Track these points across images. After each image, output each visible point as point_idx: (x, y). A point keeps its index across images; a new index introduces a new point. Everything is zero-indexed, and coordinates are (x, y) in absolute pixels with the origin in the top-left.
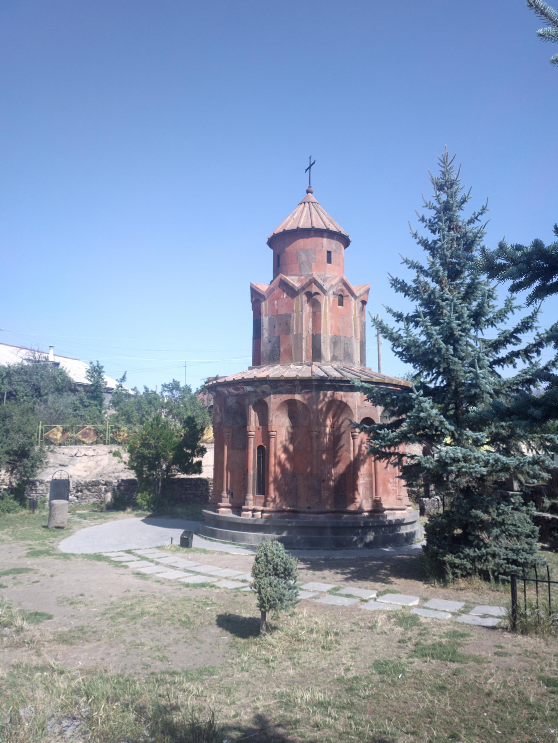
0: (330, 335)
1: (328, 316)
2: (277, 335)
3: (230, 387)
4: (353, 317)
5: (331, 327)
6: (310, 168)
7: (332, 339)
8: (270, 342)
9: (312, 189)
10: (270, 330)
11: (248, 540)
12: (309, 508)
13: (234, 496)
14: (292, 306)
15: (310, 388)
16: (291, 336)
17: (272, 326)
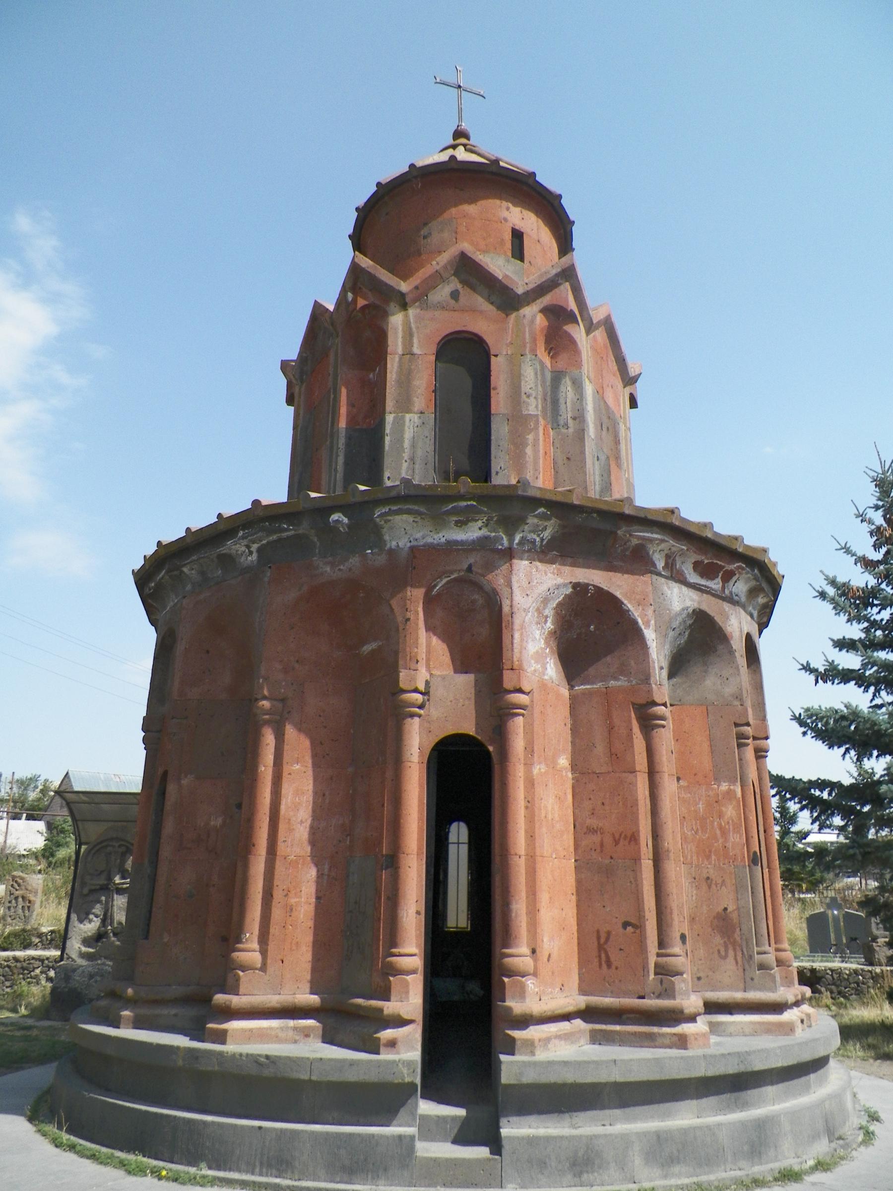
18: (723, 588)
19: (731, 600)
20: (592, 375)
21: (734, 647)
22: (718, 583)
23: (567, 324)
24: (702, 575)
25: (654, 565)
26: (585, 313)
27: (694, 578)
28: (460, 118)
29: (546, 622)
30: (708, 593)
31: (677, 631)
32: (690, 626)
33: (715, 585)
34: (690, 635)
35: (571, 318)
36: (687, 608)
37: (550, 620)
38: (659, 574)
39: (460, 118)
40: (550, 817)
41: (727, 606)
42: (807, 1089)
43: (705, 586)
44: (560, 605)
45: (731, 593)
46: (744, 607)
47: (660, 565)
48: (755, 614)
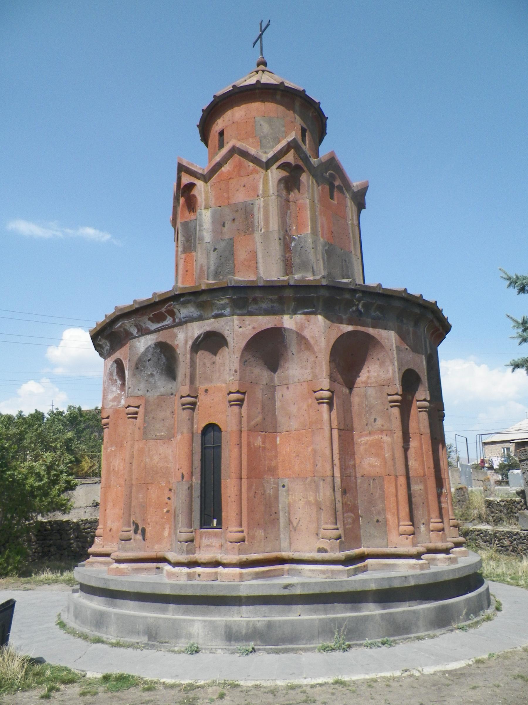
0: (322, 240)
1: (318, 209)
2: (227, 237)
3: (143, 315)
4: (350, 222)
5: (322, 227)
6: (260, 36)
7: (324, 246)
8: (215, 249)
9: (266, 59)
10: (214, 231)
11: (189, 636)
12: (320, 550)
13: (148, 535)
14: (255, 189)
15: (314, 307)
16: (257, 237)
17: (219, 223)
18: (174, 320)
19: (181, 324)
20: (212, 202)
21: (179, 352)
22: (170, 319)
23: (191, 191)
24: (158, 322)
25: (132, 334)
26: (199, 176)
27: (153, 326)
28: (262, 54)
29: (117, 382)
30: (162, 330)
31: (155, 359)
32: (161, 352)
33: (169, 321)
34: (165, 356)
35: (191, 186)
36: (150, 346)
37: (118, 380)
38: (135, 337)
39: (262, 54)
40: (116, 469)
41: (175, 330)
42: (164, 611)
43: (163, 326)
44: (117, 372)
45: (180, 319)
46: (200, 318)
47: (134, 331)
48: (228, 311)
